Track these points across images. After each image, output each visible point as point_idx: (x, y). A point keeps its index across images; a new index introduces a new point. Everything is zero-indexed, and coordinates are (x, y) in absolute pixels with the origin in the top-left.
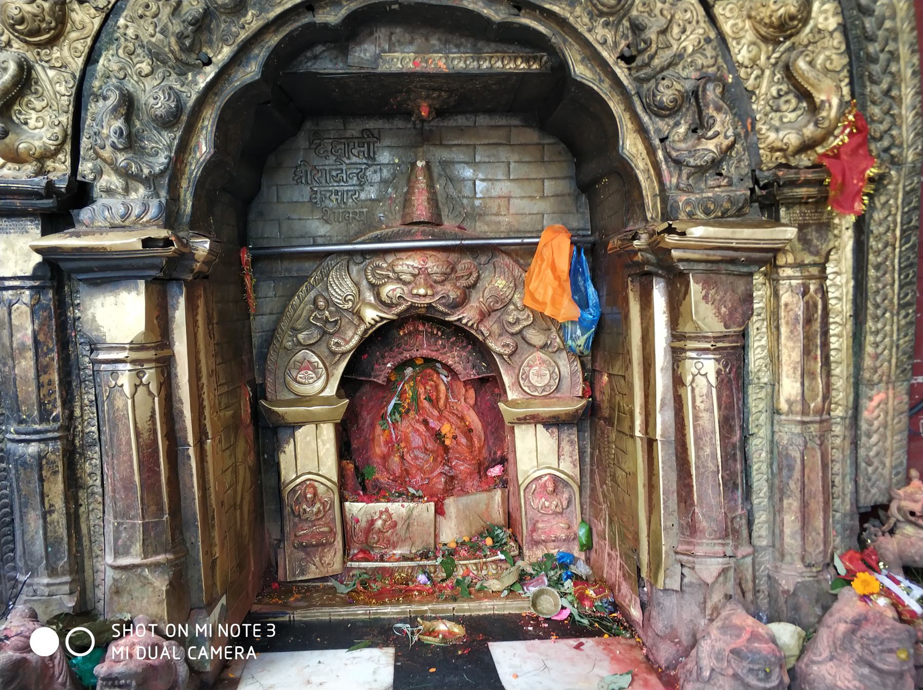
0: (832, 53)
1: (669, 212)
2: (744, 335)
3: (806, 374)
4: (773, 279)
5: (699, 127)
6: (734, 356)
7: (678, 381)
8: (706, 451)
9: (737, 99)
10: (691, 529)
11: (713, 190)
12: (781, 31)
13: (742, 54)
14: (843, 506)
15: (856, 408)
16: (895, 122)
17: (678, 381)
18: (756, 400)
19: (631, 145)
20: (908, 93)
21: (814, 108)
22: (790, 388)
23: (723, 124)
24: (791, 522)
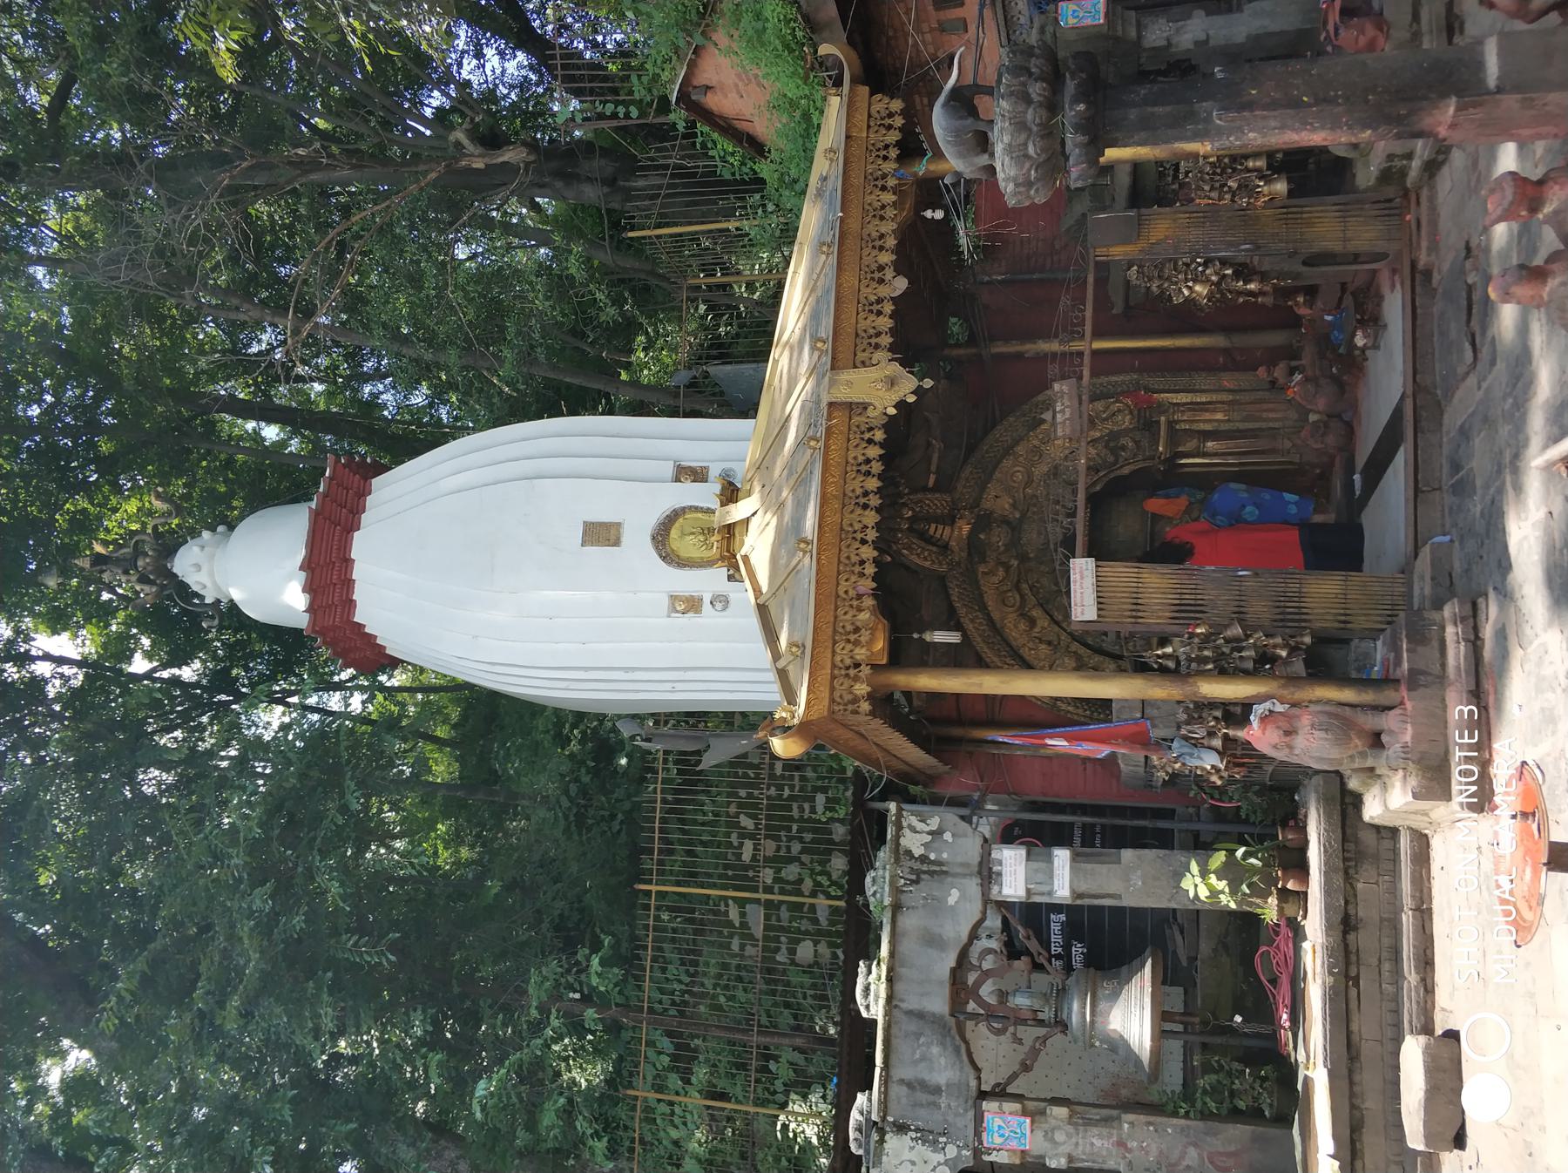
0: (1099, 405)
1: (1152, 458)
2: (1199, 432)
3: (1214, 411)
4: (1177, 422)
5: (1123, 448)
6: (1207, 435)
7: (1216, 455)
8: (1243, 445)
9: (1114, 435)
10: (1273, 451)
11: (1145, 443)
12: (1092, 422)
13: (1098, 434)
14: (1266, 395)
15: (1230, 391)
16: (1123, 382)
17: (1216, 455)
18: (1224, 427)
19: (1126, 471)
20: (1114, 378)
21: (1119, 411)
22: (1219, 416)
23: (1123, 441)
24: (1272, 415)
